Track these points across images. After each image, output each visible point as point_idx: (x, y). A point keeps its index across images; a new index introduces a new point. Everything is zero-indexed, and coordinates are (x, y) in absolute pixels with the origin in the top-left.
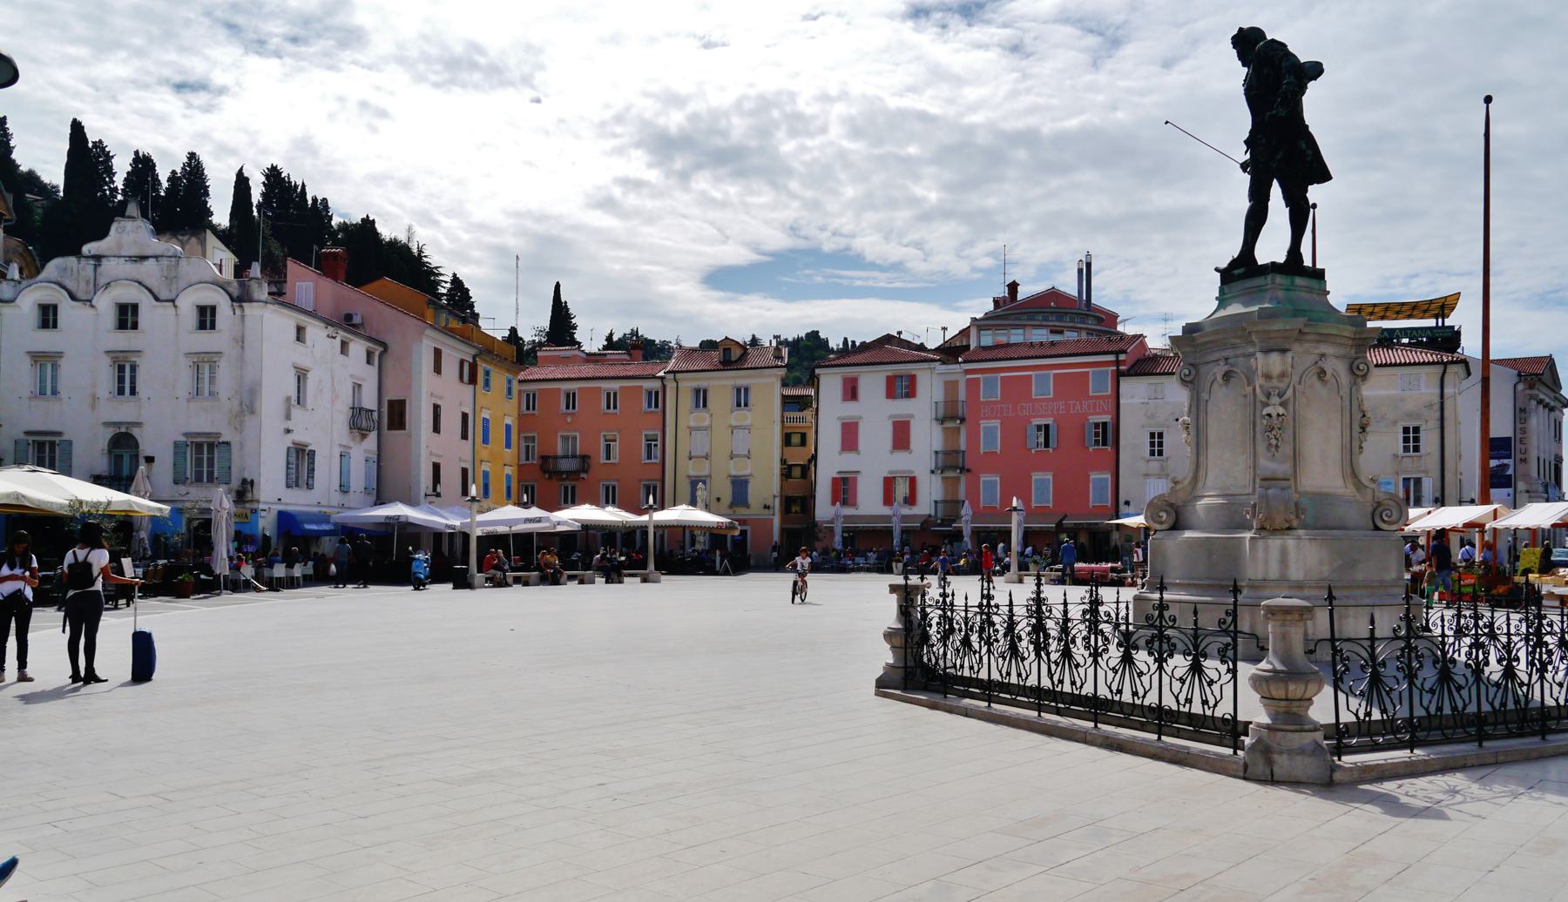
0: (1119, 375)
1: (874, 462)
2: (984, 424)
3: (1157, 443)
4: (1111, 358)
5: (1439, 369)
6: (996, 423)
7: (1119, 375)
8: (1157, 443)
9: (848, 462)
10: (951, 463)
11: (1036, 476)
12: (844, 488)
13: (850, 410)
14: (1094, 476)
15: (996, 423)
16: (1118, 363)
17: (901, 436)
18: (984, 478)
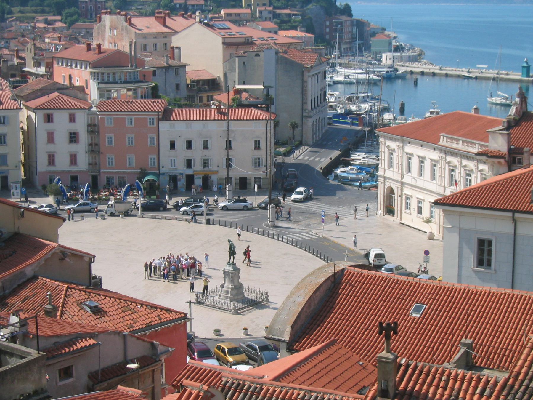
0: (159, 120)
1: (62, 149)
2: (107, 135)
3: (172, 145)
4: (156, 114)
5: (266, 121)
6: (112, 135)
7: (159, 120)
8: (172, 145)
9: (51, 148)
10: (94, 149)
11: (128, 156)
12: (51, 159)
13: (49, 126)
14: (150, 156)
15: (112, 135)
16: (158, 115)
17: (73, 138)
18: (108, 156)
